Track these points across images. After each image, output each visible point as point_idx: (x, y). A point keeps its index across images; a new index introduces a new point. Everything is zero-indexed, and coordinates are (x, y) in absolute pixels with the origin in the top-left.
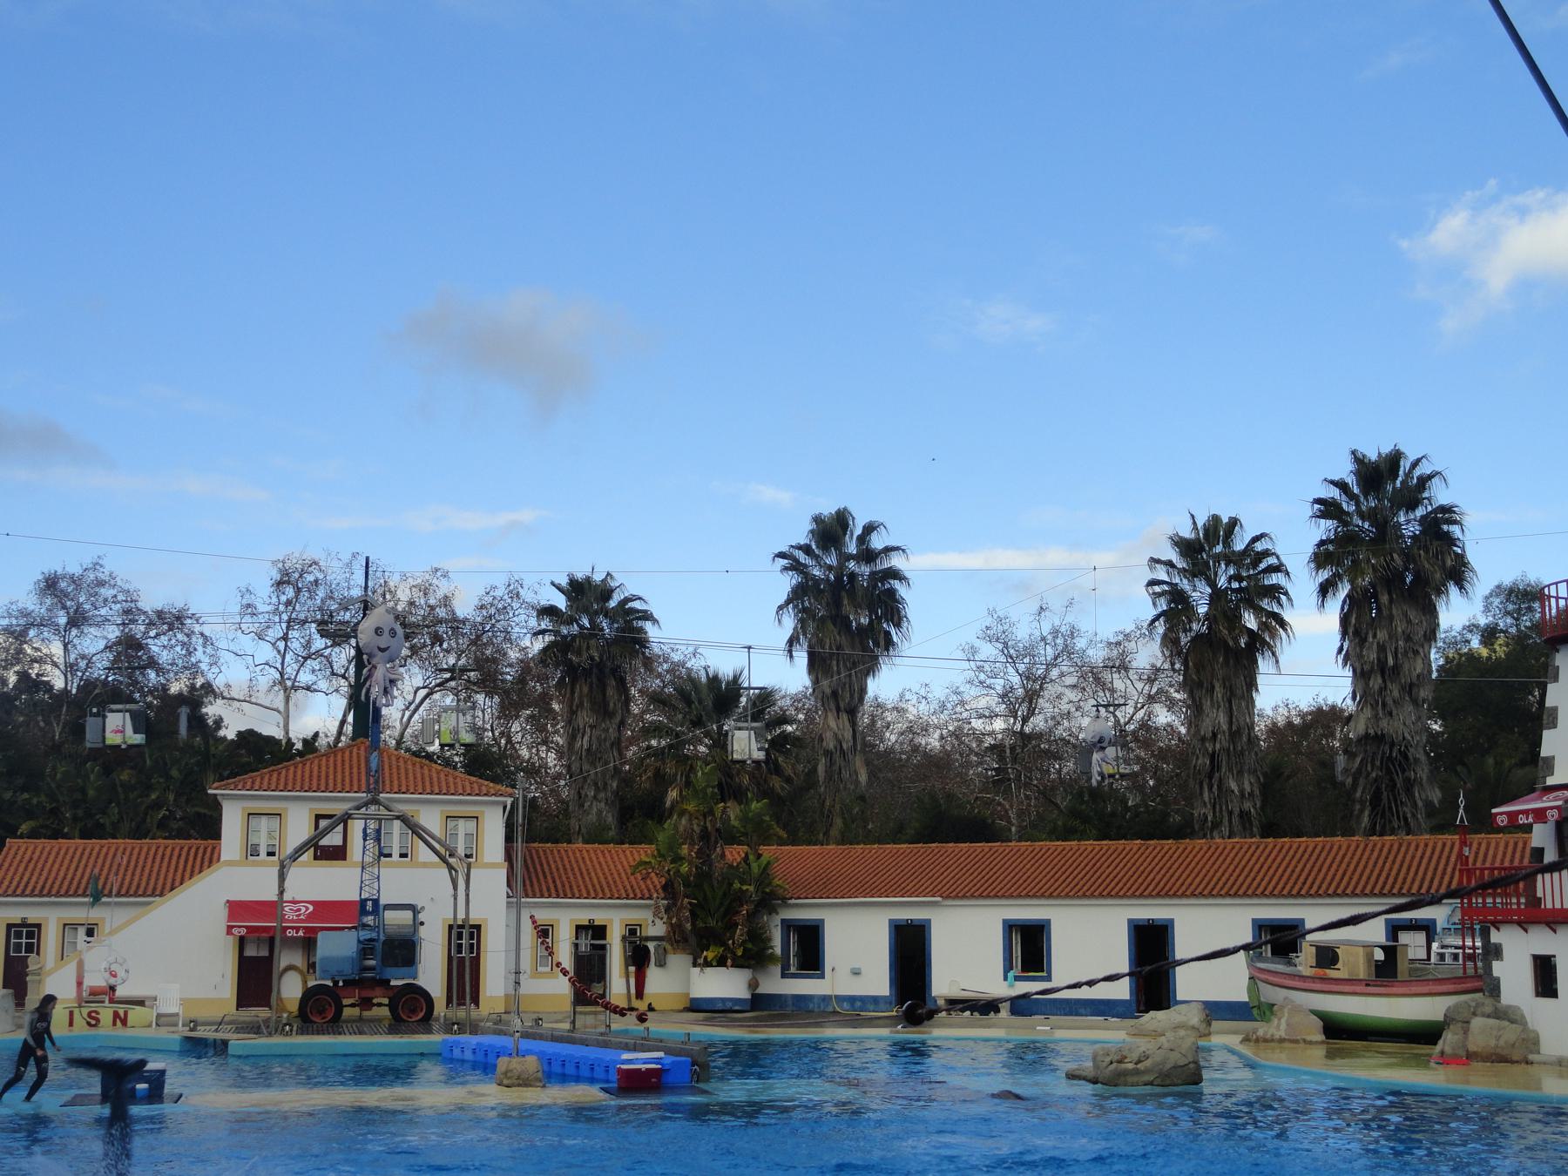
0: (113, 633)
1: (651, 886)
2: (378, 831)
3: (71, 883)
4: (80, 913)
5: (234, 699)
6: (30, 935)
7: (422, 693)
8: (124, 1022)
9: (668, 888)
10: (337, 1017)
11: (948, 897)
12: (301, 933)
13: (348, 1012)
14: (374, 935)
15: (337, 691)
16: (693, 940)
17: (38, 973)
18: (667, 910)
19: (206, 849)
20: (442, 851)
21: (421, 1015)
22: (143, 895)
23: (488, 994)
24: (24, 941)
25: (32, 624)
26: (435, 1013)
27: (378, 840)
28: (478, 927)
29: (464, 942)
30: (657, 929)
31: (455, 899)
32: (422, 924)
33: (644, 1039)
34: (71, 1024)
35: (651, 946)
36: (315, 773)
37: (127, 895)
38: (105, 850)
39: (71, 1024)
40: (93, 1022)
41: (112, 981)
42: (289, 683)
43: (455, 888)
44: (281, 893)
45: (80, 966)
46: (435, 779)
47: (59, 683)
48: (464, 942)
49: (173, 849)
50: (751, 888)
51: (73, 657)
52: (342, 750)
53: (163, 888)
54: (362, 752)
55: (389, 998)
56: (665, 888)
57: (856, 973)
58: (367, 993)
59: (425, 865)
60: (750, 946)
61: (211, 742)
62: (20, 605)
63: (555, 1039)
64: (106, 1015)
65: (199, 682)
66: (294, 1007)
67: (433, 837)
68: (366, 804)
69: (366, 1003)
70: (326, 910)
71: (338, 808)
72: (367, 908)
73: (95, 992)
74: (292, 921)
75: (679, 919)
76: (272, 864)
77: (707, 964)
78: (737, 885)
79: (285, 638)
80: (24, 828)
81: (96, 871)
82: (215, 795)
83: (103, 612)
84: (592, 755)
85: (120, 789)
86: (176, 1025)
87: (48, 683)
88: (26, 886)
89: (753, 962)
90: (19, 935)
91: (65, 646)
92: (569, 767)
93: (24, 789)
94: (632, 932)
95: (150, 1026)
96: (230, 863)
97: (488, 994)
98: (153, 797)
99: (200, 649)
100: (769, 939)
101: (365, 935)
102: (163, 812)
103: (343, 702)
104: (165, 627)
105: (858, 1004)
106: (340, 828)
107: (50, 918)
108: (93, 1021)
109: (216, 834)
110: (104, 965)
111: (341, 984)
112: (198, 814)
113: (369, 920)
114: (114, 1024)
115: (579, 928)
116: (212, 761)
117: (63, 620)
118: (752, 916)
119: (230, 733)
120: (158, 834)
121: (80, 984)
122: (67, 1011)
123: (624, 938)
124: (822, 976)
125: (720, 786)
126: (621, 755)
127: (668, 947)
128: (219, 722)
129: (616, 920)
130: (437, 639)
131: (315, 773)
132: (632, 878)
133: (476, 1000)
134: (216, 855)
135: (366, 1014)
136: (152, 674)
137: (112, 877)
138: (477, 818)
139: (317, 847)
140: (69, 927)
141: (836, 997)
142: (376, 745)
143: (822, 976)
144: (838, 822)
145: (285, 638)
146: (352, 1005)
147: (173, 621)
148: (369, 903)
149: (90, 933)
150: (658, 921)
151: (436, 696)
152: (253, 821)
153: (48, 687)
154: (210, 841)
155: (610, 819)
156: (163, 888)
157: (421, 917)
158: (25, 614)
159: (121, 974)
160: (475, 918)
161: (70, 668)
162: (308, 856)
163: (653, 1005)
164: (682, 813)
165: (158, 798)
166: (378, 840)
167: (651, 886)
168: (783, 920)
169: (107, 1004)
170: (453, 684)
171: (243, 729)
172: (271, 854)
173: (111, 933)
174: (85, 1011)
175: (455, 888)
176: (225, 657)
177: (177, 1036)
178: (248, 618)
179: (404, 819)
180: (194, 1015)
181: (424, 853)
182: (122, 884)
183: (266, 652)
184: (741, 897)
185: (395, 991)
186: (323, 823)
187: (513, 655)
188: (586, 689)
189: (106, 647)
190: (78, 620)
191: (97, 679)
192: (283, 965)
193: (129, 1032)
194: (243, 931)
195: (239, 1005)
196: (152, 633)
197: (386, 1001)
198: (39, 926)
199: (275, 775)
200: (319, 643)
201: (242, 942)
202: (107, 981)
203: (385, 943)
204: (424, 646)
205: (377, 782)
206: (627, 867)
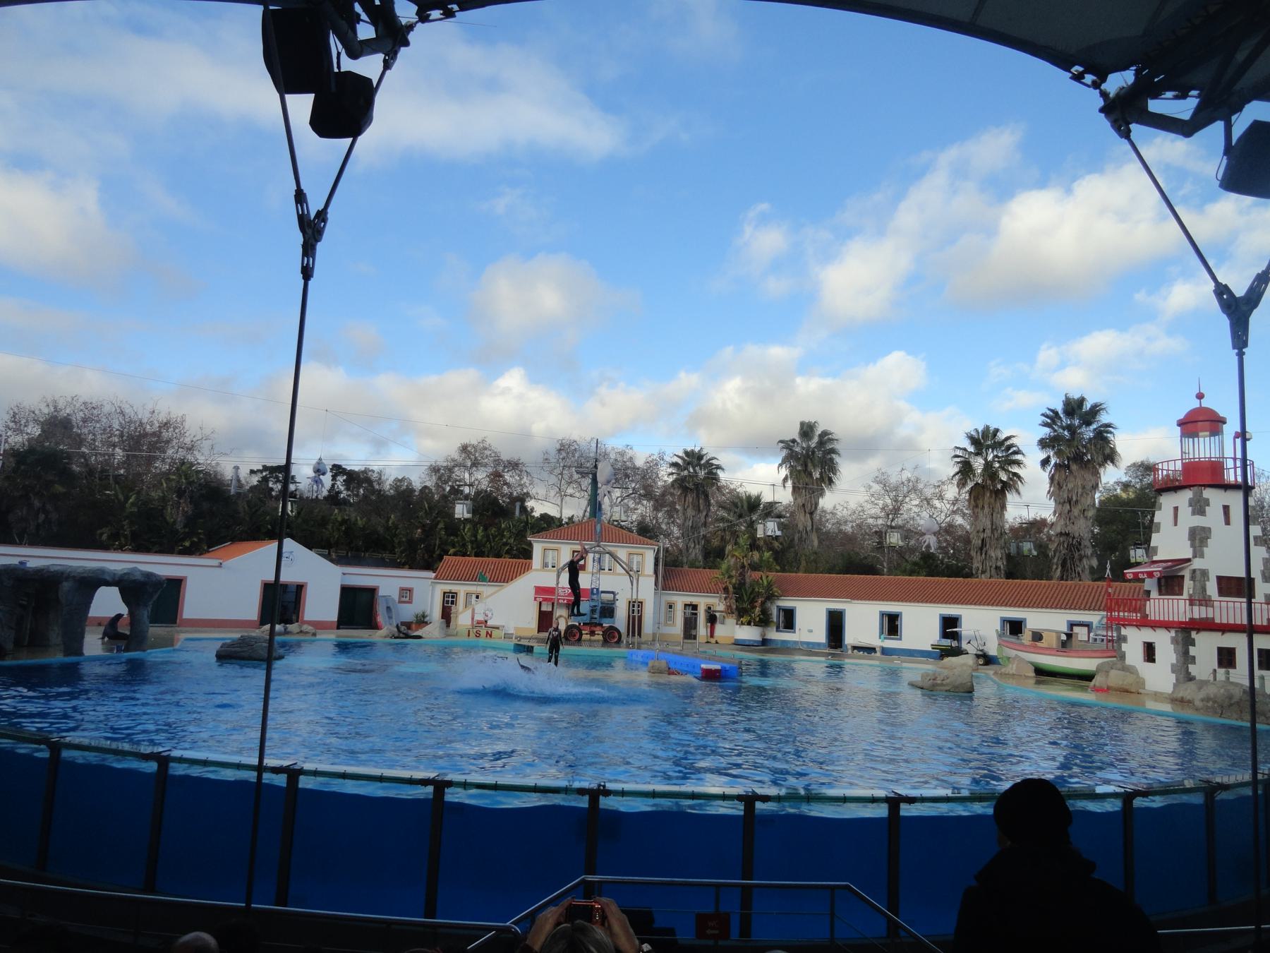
0: (490, 470)
2: (600, 559)
6: (453, 597)
7: (619, 499)
8: (491, 636)
9: (726, 590)
10: (580, 639)
11: (854, 599)
12: (565, 602)
13: (584, 637)
16: (736, 613)
17: (456, 613)
20: (627, 569)
21: (616, 640)
22: (500, 582)
24: (450, 599)
25: (457, 465)
27: (599, 562)
28: (642, 603)
29: (635, 609)
30: (719, 605)
31: (632, 589)
33: (714, 656)
34: (469, 635)
35: (717, 614)
37: (493, 581)
39: (469, 635)
41: (486, 618)
42: (563, 493)
43: (632, 585)
44: (558, 584)
45: (473, 610)
48: (635, 609)
50: (763, 591)
51: (473, 479)
53: (508, 579)
57: (811, 631)
58: (593, 629)
59: (619, 574)
60: (761, 616)
62: (452, 457)
64: (483, 632)
65: (525, 491)
67: (623, 562)
68: (595, 547)
69: (592, 633)
73: (479, 622)
76: (554, 571)
77: (742, 624)
78: (757, 590)
79: (561, 474)
80: (452, 551)
84: (694, 528)
85: (491, 537)
86: (512, 638)
89: (763, 624)
91: (470, 475)
92: (683, 535)
94: (709, 608)
98: (505, 540)
99: (525, 477)
100: (771, 614)
101: (593, 604)
103: (586, 502)
104: (511, 468)
105: (811, 646)
107: (462, 589)
112: (523, 548)
113: (595, 597)
114: (487, 636)
115: (686, 605)
117: (469, 464)
118: (763, 603)
119: (536, 514)
120: (506, 556)
121: (473, 619)
123: (706, 611)
124: (795, 632)
125: (750, 545)
128: (532, 510)
129: (702, 601)
130: (627, 476)
133: (640, 634)
135: (592, 638)
140: (468, 595)
141: (801, 642)
142: (600, 521)
143: (795, 632)
144: (804, 563)
145: (561, 474)
146: (587, 634)
147: (514, 465)
148: (595, 590)
149: (477, 597)
151: (626, 501)
155: (700, 558)
156: (508, 579)
157: (617, 597)
158: (453, 460)
160: (640, 598)
163: (718, 641)
164: (733, 556)
165: (507, 541)
166: (599, 562)
168: (777, 606)
170: (633, 495)
172: (553, 567)
174: (475, 630)
175: (632, 585)
177: (512, 644)
180: (518, 635)
181: (619, 569)
183: (553, 479)
184: (759, 594)
186: (576, 554)
188: (691, 500)
191: (482, 490)
192: (558, 615)
193: (492, 641)
194: (541, 600)
195: (538, 632)
196: (506, 470)
197: (601, 633)
198: (456, 593)
199: (556, 533)
200: (576, 476)
201: (540, 603)
203: (601, 607)
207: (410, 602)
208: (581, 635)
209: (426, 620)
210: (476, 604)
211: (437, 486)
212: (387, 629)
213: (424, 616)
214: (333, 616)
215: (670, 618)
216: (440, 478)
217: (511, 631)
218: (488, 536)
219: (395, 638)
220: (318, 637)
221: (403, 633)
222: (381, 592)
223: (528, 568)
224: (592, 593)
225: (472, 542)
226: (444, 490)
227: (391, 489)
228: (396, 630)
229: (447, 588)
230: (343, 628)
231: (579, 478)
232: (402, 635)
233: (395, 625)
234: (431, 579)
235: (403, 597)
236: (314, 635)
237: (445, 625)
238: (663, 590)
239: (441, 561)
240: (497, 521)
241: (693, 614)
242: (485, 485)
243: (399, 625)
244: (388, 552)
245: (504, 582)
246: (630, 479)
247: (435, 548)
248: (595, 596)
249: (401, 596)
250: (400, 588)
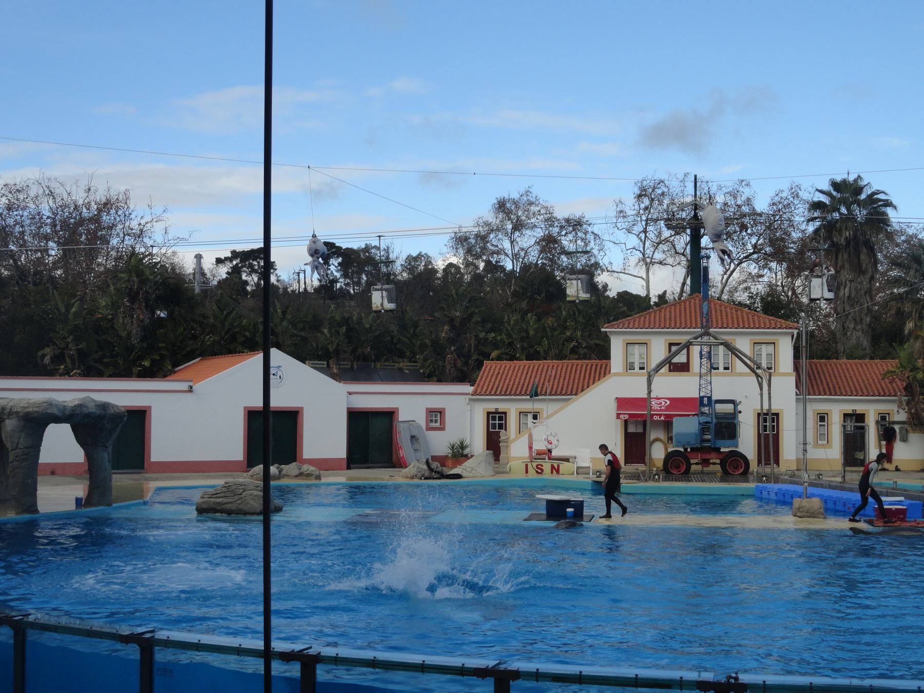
0: (539, 233)
1: (896, 388)
2: (710, 353)
3: (522, 388)
4: (528, 406)
5: (614, 272)
6: (500, 419)
8: (558, 471)
9: (908, 389)
10: (687, 471)
12: (662, 418)
13: (693, 468)
14: (709, 419)
15: (679, 264)
17: (506, 441)
18: (908, 403)
19: (602, 365)
21: (741, 470)
22: (566, 394)
23: (785, 458)
24: (497, 422)
25: (492, 230)
26: (751, 469)
27: (710, 358)
28: (777, 415)
29: (768, 424)
30: (900, 416)
31: (762, 396)
32: (740, 412)
34: (527, 472)
35: (897, 427)
36: (668, 316)
37: (556, 394)
38: (541, 367)
39: (527, 472)
40: (539, 471)
41: (549, 446)
42: (648, 260)
43: (761, 389)
44: (649, 392)
45: (530, 437)
46: (746, 319)
47: (509, 266)
48: (768, 424)
49: (582, 366)
51: (517, 249)
52: (684, 301)
53: (577, 390)
54: (697, 302)
55: (721, 460)
56: (906, 389)
58: (706, 456)
59: (741, 374)
61: (602, 299)
62: (484, 219)
63: (831, 487)
64: (547, 467)
65: (592, 262)
66: (660, 464)
68: (701, 336)
69: (706, 462)
70: (677, 403)
71: (683, 339)
72: (703, 402)
73: (539, 453)
74: (657, 410)
75: (916, 410)
76: (643, 375)
79: (645, 231)
80: (494, 354)
81: (537, 380)
82: (606, 332)
83: (533, 220)
85: (548, 330)
86: (589, 474)
87: (502, 267)
88: (497, 390)
90: (494, 419)
91: (512, 242)
92: (835, 309)
93: (490, 331)
94: (883, 418)
95: (573, 474)
96: (617, 374)
97: (785, 458)
98: (568, 333)
101: (703, 419)
102: (574, 343)
103: (684, 271)
104: (571, 228)
106: (685, 351)
107: (512, 409)
108: (540, 470)
109: (608, 357)
110: (544, 437)
111: (689, 450)
112: (596, 345)
113: (706, 410)
114: (552, 472)
115: (846, 416)
116: (603, 310)
117: (509, 226)
119: (612, 294)
120: (572, 356)
121: (531, 448)
122: (524, 464)
123: (877, 422)
126: (872, 299)
127: (909, 429)
128: (605, 287)
129: (872, 411)
131: (668, 316)
132: (882, 382)
133: (777, 462)
134: (607, 372)
135: (705, 469)
136: (564, 258)
137: (546, 383)
138: (774, 343)
139: (670, 364)
142: (706, 297)
145: (645, 231)
146: (697, 464)
147: (576, 224)
148: (706, 399)
150: (901, 411)
151: (744, 265)
152: (630, 348)
153: (503, 269)
154: (604, 361)
155: (866, 343)
156: (577, 390)
157: (740, 408)
158: (487, 224)
159: (555, 442)
160: (775, 408)
161: (515, 257)
162: (665, 370)
163: (899, 467)
164: (917, 338)
165: (571, 335)
166: (710, 358)
167: (896, 388)
169: (547, 460)
170: (755, 256)
171: (621, 291)
173: (548, 417)
174: (535, 464)
175: (761, 389)
176: (608, 245)
177: (590, 481)
178: (621, 220)
179: (727, 345)
181: (740, 367)
182: (552, 388)
183: (633, 241)
185: (724, 455)
186: (674, 348)
187: (795, 235)
188: (846, 256)
189: (536, 242)
190: (518, 226)
191: (532, 263)
192: (652, 437)
193: (561, 477)
194: (627, 417)
196: (563, 233)
197: (718, 461)
198: (505, 413)
199: (642, 318)
200: (666, 233)
201: (626, 422)
204: (735, 232)
205: (707, 321)
206: (879, 375)
207: (442, 428)
208: (689, 465)
209: (466, 451)
210: (535, 427)
211: (468, 264)
212: (414, 467)
213: (462, 446)
214: (340, 451)
215: (824, 437)
216: (469, 251)
217: (587, 465)
218: (544, 329)
219: (426, 478)
220: (324, 480)
221: (438, 472)
222: (402, 417)
223: (605, 372)
224: (702, 404)
225: (522, 340)
226: (477, 267)
227: (403, 270)
228: (425, 467)
229: (492, 407)
231: (671, 236)
233: (425, 461)
234: (468, 394)
235: (431, 421)
236: (318, 477)
237: (492, 459)
238: (809, 394)
239: (480, 370)
240: (554, 306)
241: (857, 428)
242: (534, 256)
243: (430, 460)
244: (405, 360)
245: (571, 394)
246: (749, 231)
247: (470, 351)
248: (707, 408)
249: (429, 420)
250: (427, 409)
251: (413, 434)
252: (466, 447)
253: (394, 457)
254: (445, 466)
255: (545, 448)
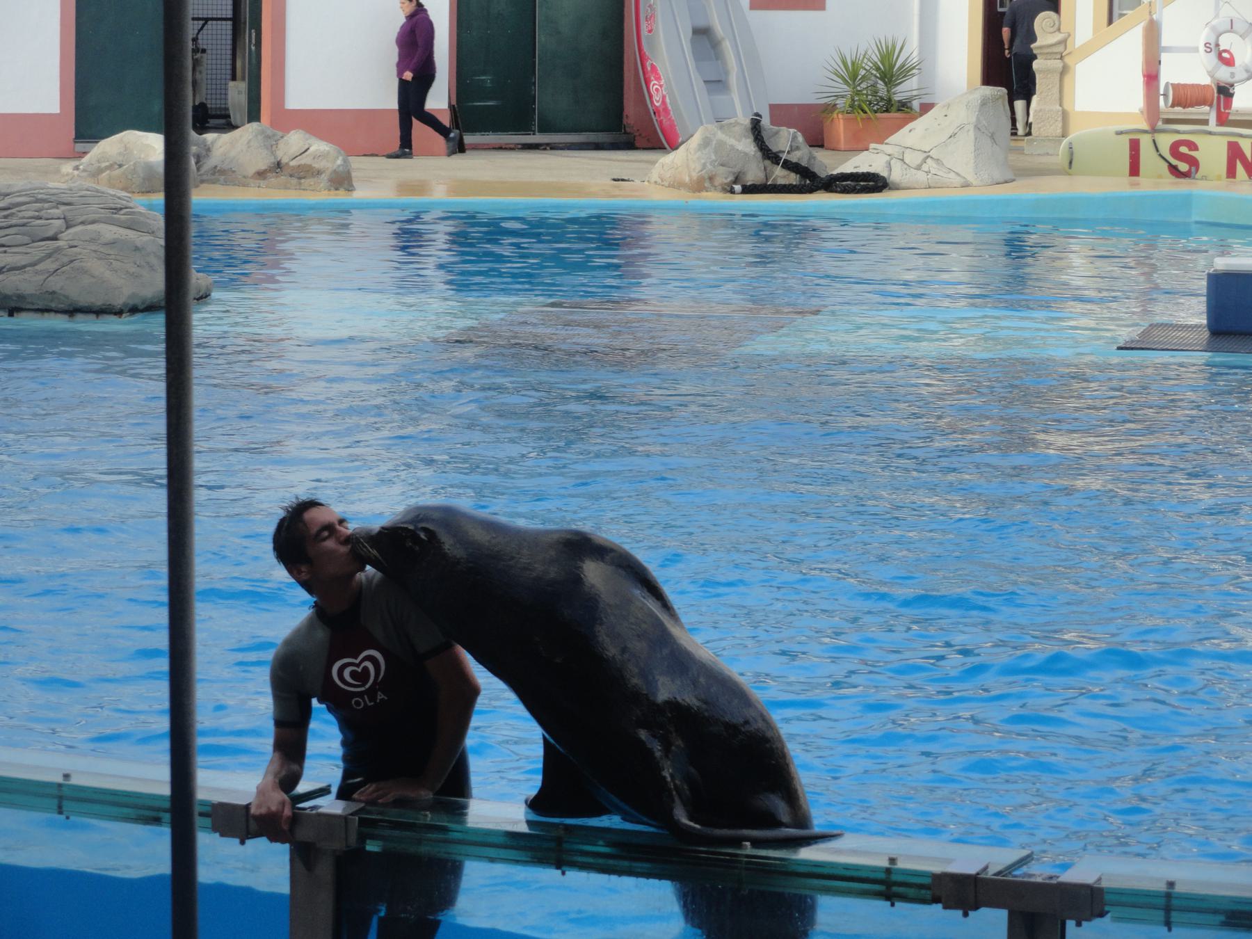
17: (1061, 51)
34: (1134, 170)
39: (1134, 170)
40: (1183, 167)
41: (1224, 74)
45: (1152, 34)
64: (1213, 152)
73: (1185, 97)
114: (1231, 172)
121: (1151, 78)
122: (1125, 140)
169: (1213, 125)
174: (1166, 141)
202: (1211, 75)
212: (706, 143)
213: (890, 72)
219: (749, 190)
221: (790, 166)
228: (748, 146)
230: (476, 147)
232: (781, 175)
233: (746, 122)
236: (342, 181)
243: (766, 122)
251: (701, 23)
252: (906, 72)
253: (630, 108)
254: (822, 146)
255: (1204, 80)
